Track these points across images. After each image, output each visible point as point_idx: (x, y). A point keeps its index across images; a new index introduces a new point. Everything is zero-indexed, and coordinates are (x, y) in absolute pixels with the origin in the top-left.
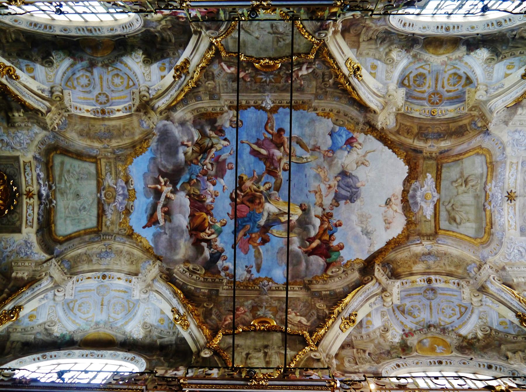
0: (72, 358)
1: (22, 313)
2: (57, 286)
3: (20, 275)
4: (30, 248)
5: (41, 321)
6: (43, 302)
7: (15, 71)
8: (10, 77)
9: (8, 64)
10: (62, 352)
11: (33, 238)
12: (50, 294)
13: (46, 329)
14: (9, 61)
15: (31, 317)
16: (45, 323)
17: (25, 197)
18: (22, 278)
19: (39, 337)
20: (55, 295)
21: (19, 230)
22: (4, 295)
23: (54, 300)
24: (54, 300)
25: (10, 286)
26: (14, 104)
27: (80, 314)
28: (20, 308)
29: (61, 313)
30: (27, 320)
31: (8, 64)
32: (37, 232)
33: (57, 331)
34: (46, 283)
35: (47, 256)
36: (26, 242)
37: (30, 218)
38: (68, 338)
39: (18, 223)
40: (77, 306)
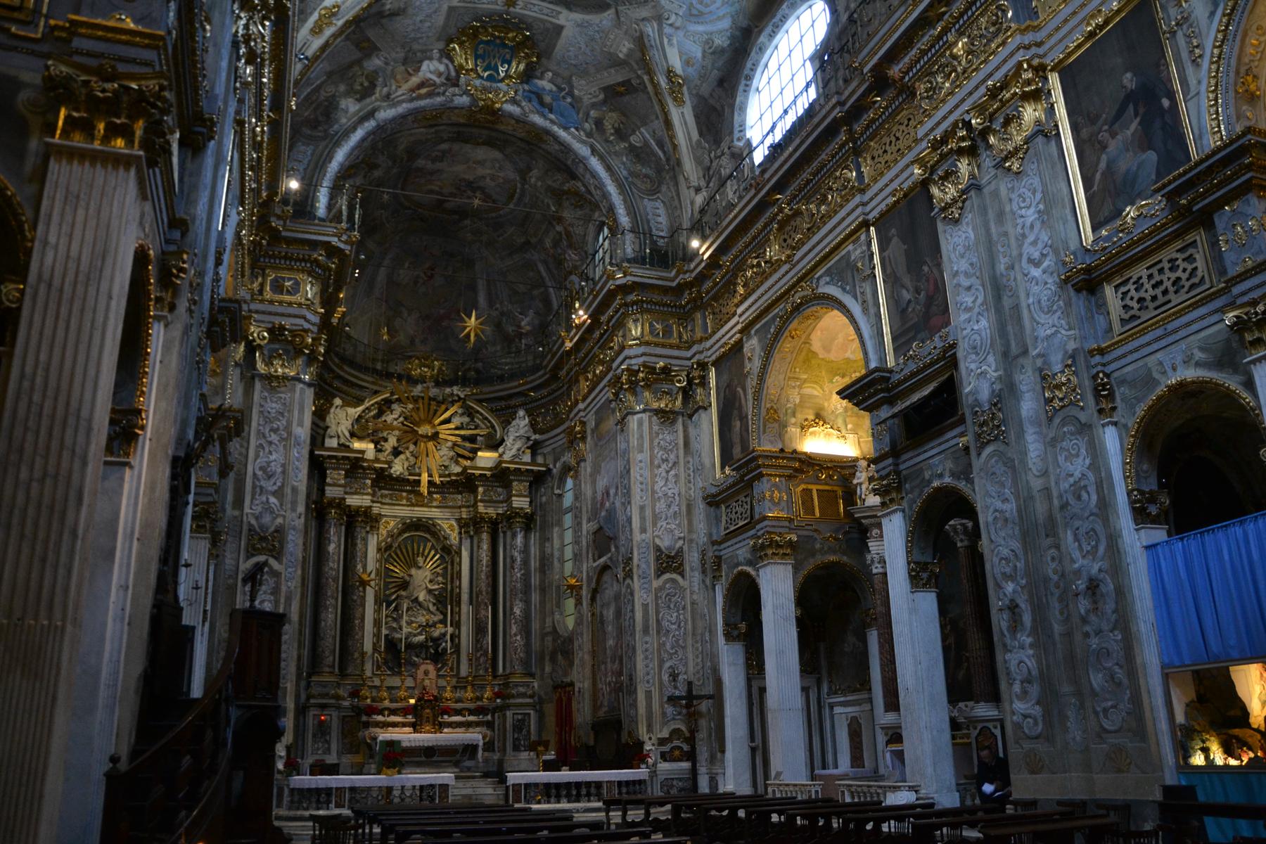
0: (766, 49)
1: (679, 70)
2: (659, 18)
3: (625, 50)
4: (591, 25)
5: (699, 55)
6: (675, 42)
7: (325, 8)
8: (334, 14)
9: (315, 16)
10: (753, 54)
11: (577, 17)
12: (667, 30)
13: (713, 53)
14: (311, 14)
15: (687, 63)
16: (704, 52)
17: (512, 9)
18: (630, 50)
19: (720, 63)
20: (671, 25)
21: (560, 29)
22: (646, 78)
23: (677, 28)
24: (677, 28)
25: (636, 67)
26: (374, 10)
27: (712, 8)
28: (669, 71)
29: (701, 28)
30: (690, 70)
31: (315, 16)
32: (570, 10)
33: (721, 41)
34: (650, 30)
35: (611, 11)
36: (578, 25)
37: (545, 11)
38: (738, 33)
39: (548, 25)
40: (699, 6)
